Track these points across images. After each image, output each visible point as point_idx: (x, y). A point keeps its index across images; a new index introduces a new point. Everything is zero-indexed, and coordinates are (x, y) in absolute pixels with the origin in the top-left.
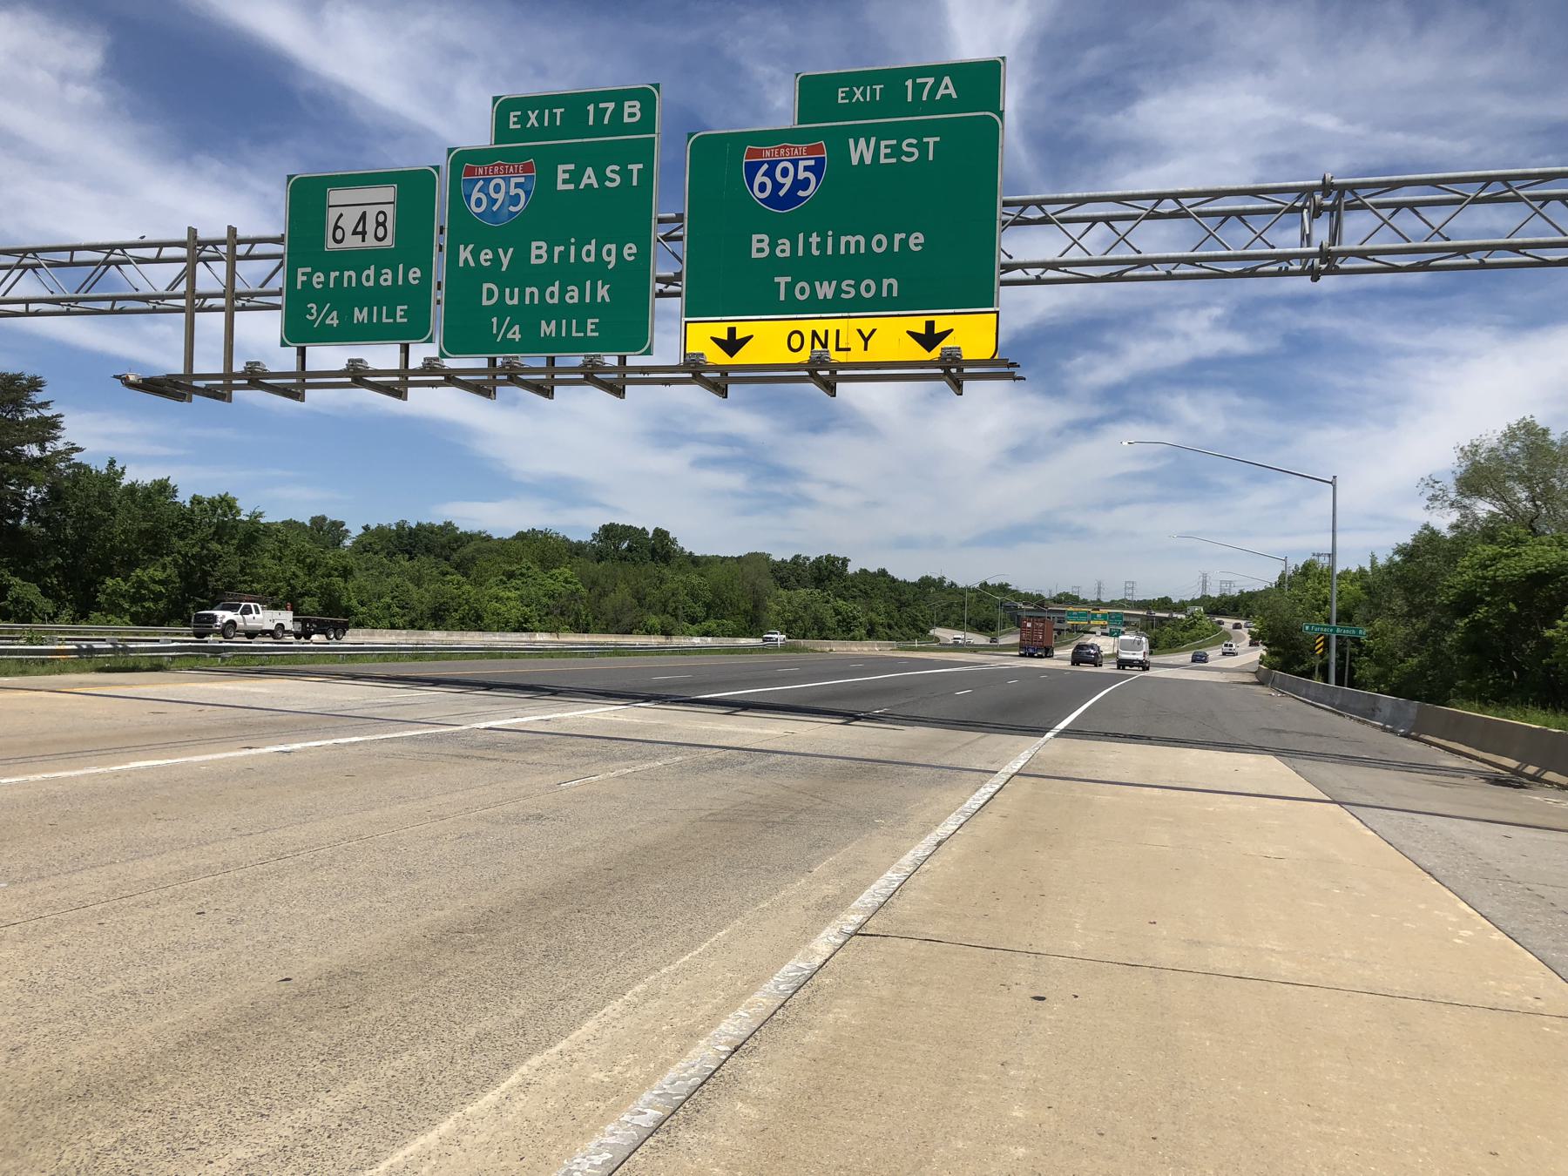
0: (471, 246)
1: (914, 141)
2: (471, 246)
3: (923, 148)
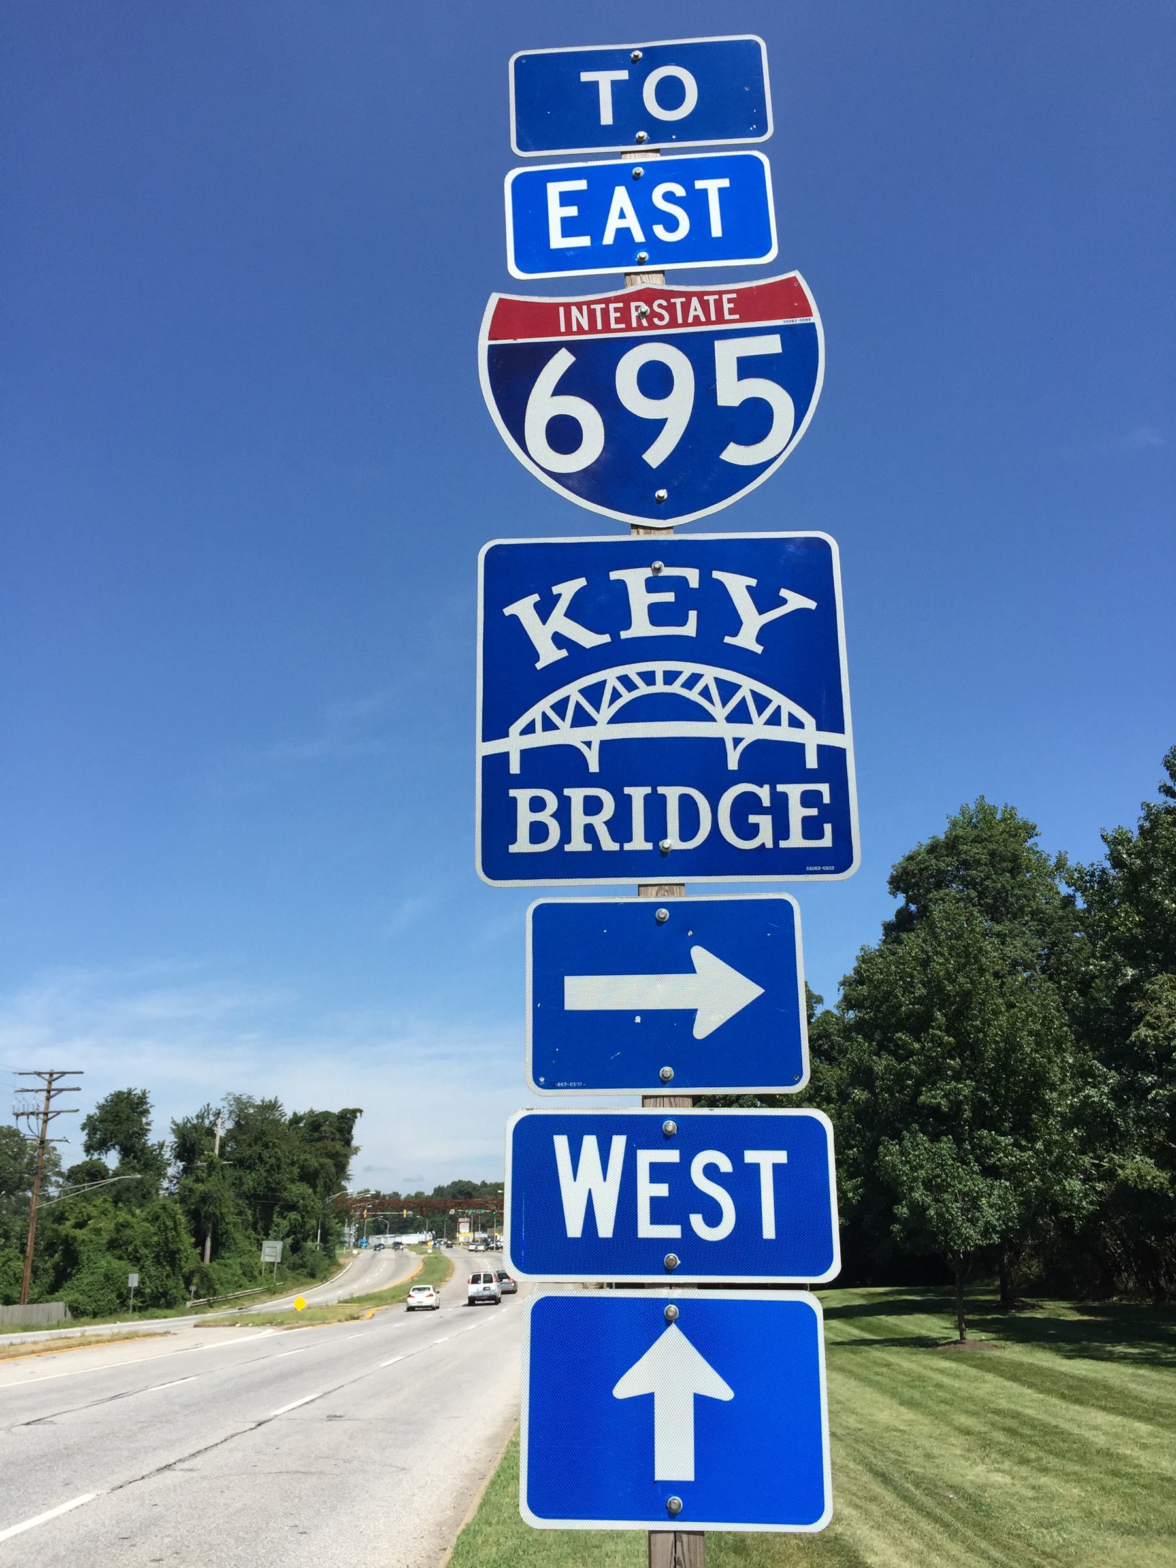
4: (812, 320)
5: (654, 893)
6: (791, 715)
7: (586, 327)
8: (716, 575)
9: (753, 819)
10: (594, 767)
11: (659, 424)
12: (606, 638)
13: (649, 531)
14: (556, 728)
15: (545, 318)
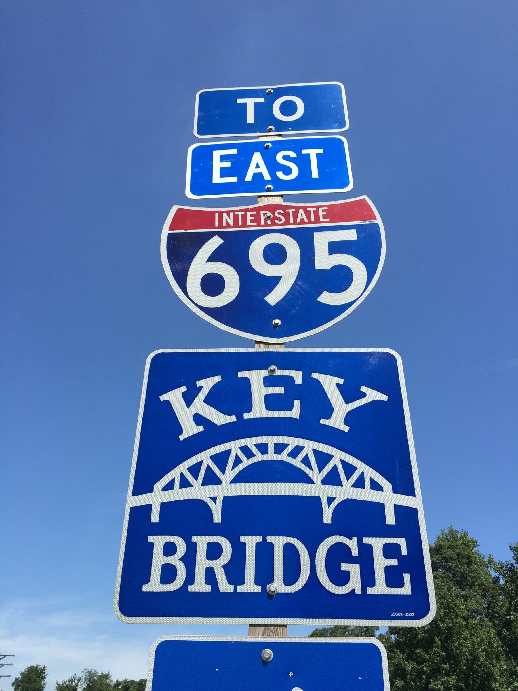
4: (376, 222)
5: (261, 633)
6: (372, 481)
7: (231, 224)
8: (314, 375)
9: (344, 567)
10: (217, 518)
11: (276, 280)
12: (233, 419)
13: (267, 345)
14: (190, 486)
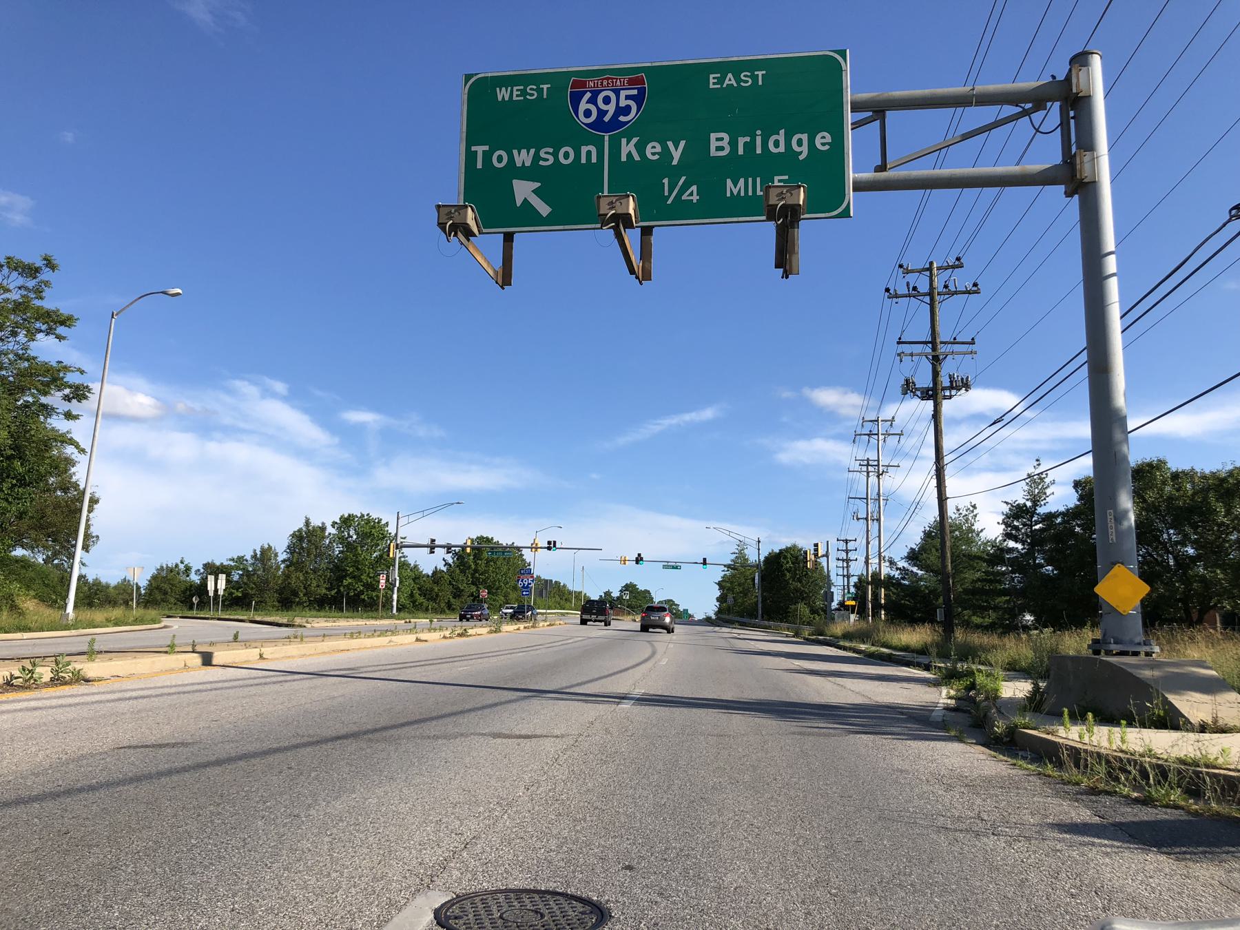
0: (635, 140)
1: (535, 87)
2: (635, 140)
3: (540, 91)
15: (583, 84)
